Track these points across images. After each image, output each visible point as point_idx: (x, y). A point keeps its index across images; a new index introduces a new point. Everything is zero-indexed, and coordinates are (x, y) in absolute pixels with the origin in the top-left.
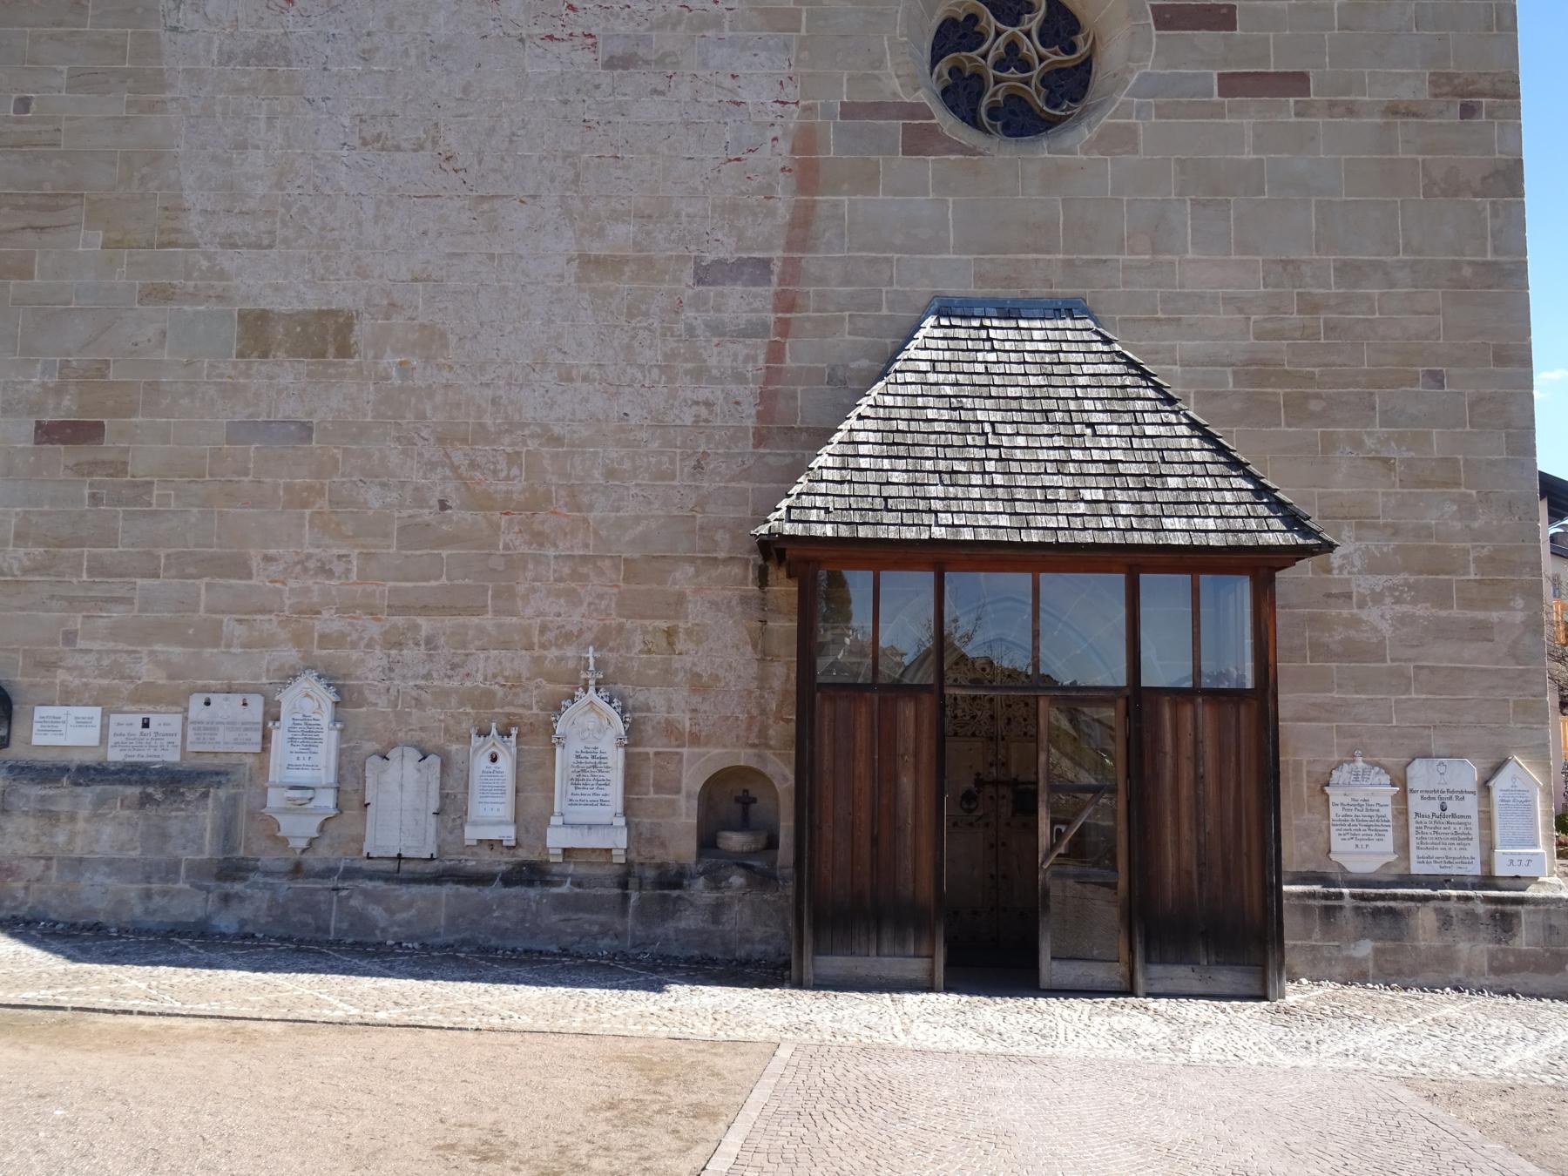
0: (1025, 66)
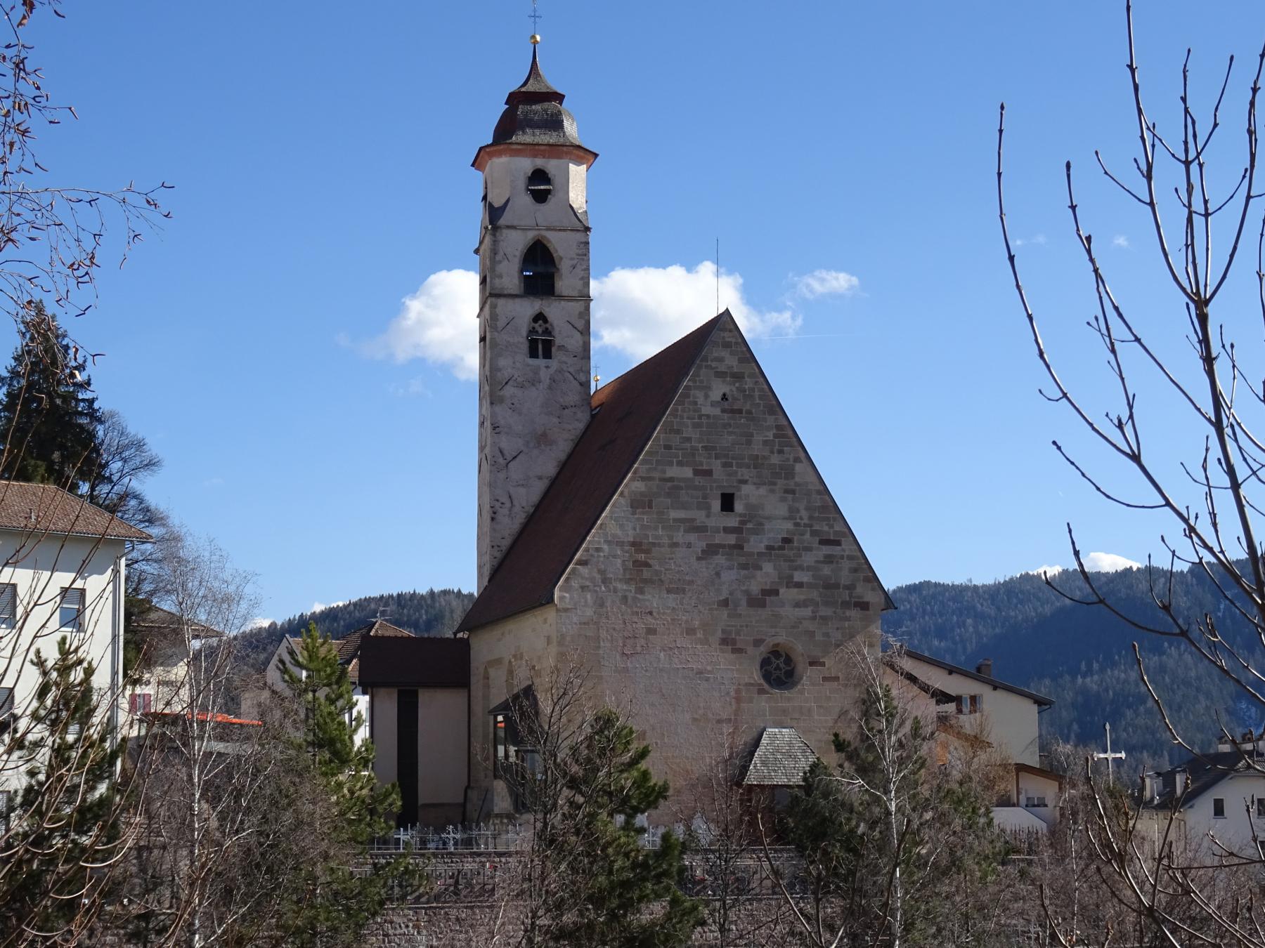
0: (780, 670)
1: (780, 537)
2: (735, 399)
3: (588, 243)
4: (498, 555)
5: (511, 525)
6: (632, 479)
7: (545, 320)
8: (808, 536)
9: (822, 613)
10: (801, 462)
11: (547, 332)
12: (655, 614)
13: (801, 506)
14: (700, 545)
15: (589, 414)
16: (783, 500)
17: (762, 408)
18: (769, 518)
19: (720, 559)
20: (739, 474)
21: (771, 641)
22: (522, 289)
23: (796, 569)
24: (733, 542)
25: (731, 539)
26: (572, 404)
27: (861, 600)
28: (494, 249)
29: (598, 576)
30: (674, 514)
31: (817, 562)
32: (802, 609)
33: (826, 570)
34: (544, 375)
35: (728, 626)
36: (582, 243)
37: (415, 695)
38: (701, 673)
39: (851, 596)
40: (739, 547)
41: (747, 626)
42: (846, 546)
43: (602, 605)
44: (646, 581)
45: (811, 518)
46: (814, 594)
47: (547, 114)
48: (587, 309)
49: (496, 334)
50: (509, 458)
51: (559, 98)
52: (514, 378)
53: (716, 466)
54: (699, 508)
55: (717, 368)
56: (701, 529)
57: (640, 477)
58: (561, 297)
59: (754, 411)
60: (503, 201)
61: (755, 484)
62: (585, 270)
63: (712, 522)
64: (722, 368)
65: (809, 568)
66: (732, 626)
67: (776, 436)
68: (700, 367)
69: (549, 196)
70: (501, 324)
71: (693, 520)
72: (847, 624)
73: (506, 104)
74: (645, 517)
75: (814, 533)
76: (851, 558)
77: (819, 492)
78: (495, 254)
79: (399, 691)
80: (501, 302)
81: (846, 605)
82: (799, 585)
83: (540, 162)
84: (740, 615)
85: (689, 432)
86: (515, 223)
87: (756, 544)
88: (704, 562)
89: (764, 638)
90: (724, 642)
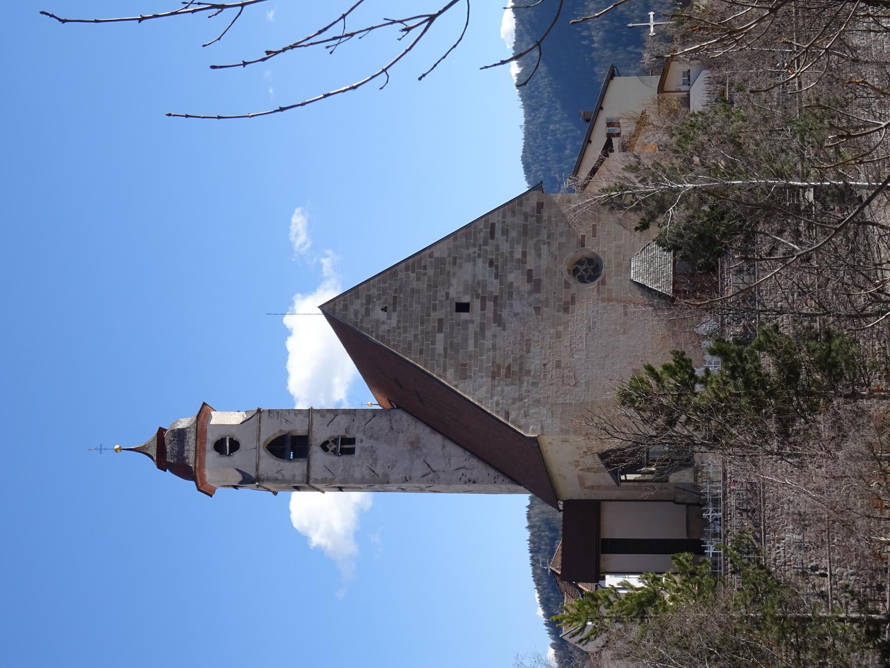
1: (488, 268)
2: (386, 300)
3: (269, 410)
4: (501, 478)
5: (479, 469)
6: (445, 378)
7: (327, 442)
8: (488, 248)
9: (546, 236)
10: (432, 253)
11: (335, 441)
12: (545, 362)
13: (465, 252)
14: (493, 329)
15: (397, 410)
16: (461, 266)
17: (392, 282)
18: (474, 277)
19: (505, 313)
20: (441, 298)
21: (566, 275)
22: (303, 459)
23: (512, 257)
24: (492, 303)
25: (490, 305)
26: (388, 423)
27: (536, 208)
28: (273, 480)
29: (518, 404)
30: (471, 347)
31: (507, 241)
32: (542, 252)
33: (513, 234)
34: (367, 444)
35: (554, 306)
36: (269, 415)
37: (605, 541)
38: (589, 327)
39: (532, 216)
40: (496, 298)
41: (555, 293)
42: (494, 219)
43: (539, 401)
44: (521, 369)
45: (474, 245)
46: (531, 243)
47: (173, 440)
48: (318, 411)
49: (336, 479)
50: (428, 470)
51: (161, 431)
52: (370, 466)
53: (435, 315)
54: (467, 329)
55: (362, 315)
56: (483, 327)
57: (443, 372)
58: (309, 431)
59: (394, 288)
60: (238, 473)
61: (449, 287)
62: (289, 413)
63: (477, 319)
64: (363, 311)
65: (512, 247)
66: (554, 303)
67: (413, 272)
68: (362, 328)
69: (234, 439)
70: (329, 476)
71: (475, 333)
72: (553, 219)
73: (165, 471)
74: (473, 369)
75: (486, 243)
76: (504, 216)
77: (455, 239)
78: (277, 479)
79: (603, 552)
80: (313, 475)
81: (539, 220)
82: (524, 254)
83: (209, 446)
84: (546, 298)
85: (410, 336)
86: (254, 464)
87: (494, 286)
88: (507, 325)
89: (563, 281)
90: (566, 310)
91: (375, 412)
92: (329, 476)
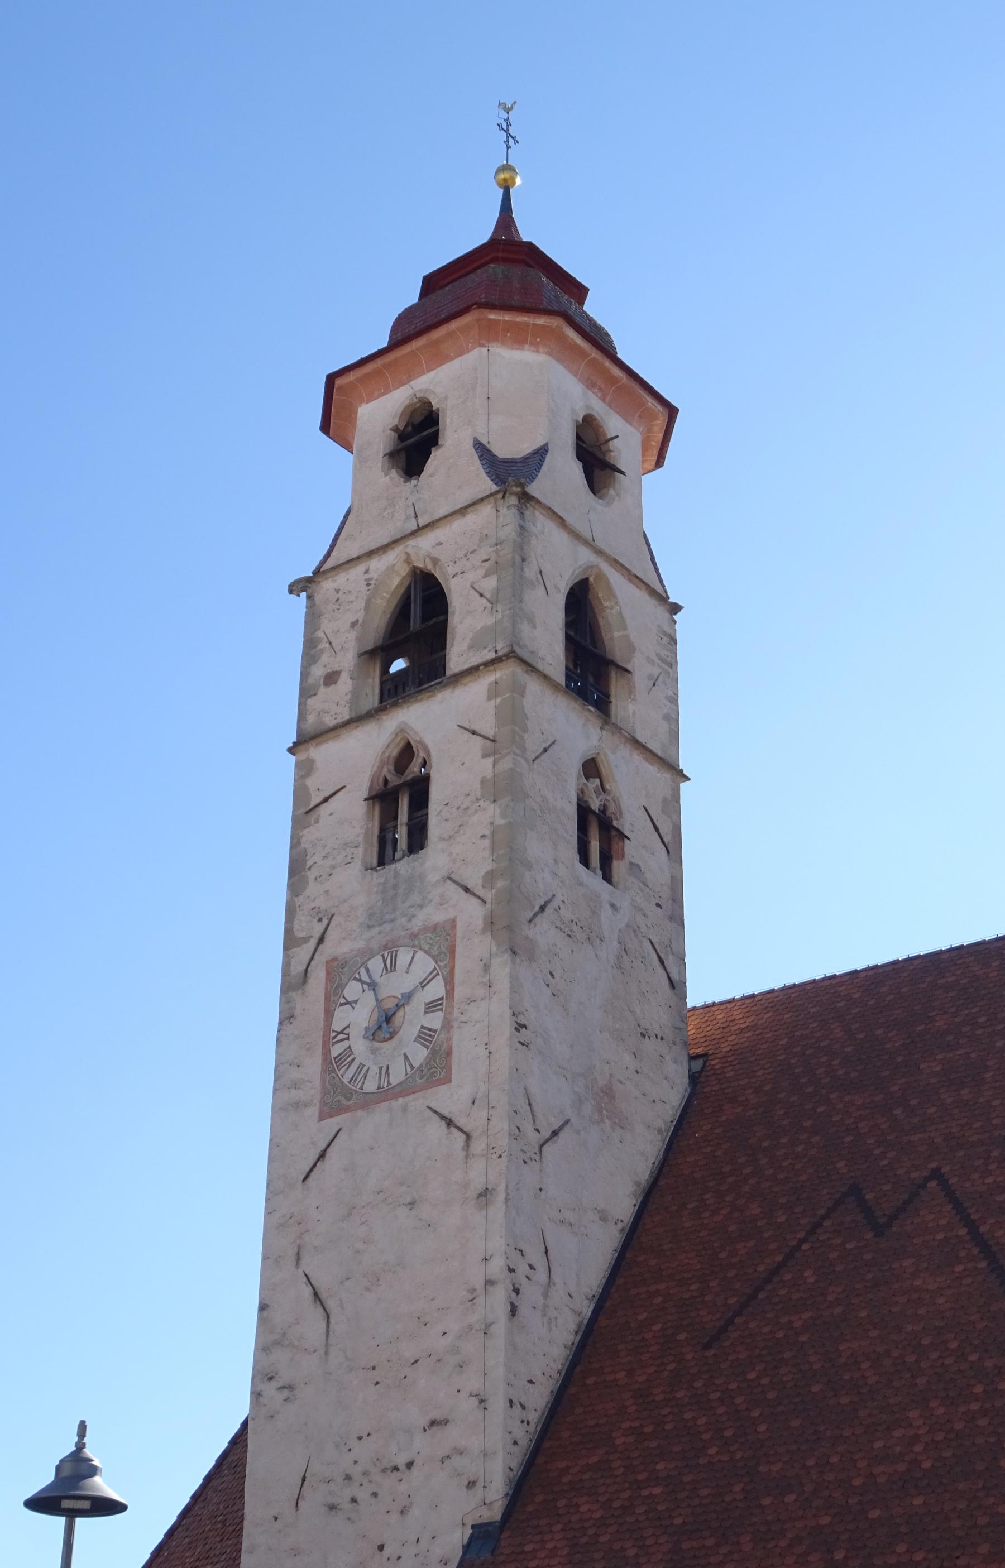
34: (610, 923)
52: (555, 904)
83: (599, 408)
91: (677, 986)
92: (533, 743)
